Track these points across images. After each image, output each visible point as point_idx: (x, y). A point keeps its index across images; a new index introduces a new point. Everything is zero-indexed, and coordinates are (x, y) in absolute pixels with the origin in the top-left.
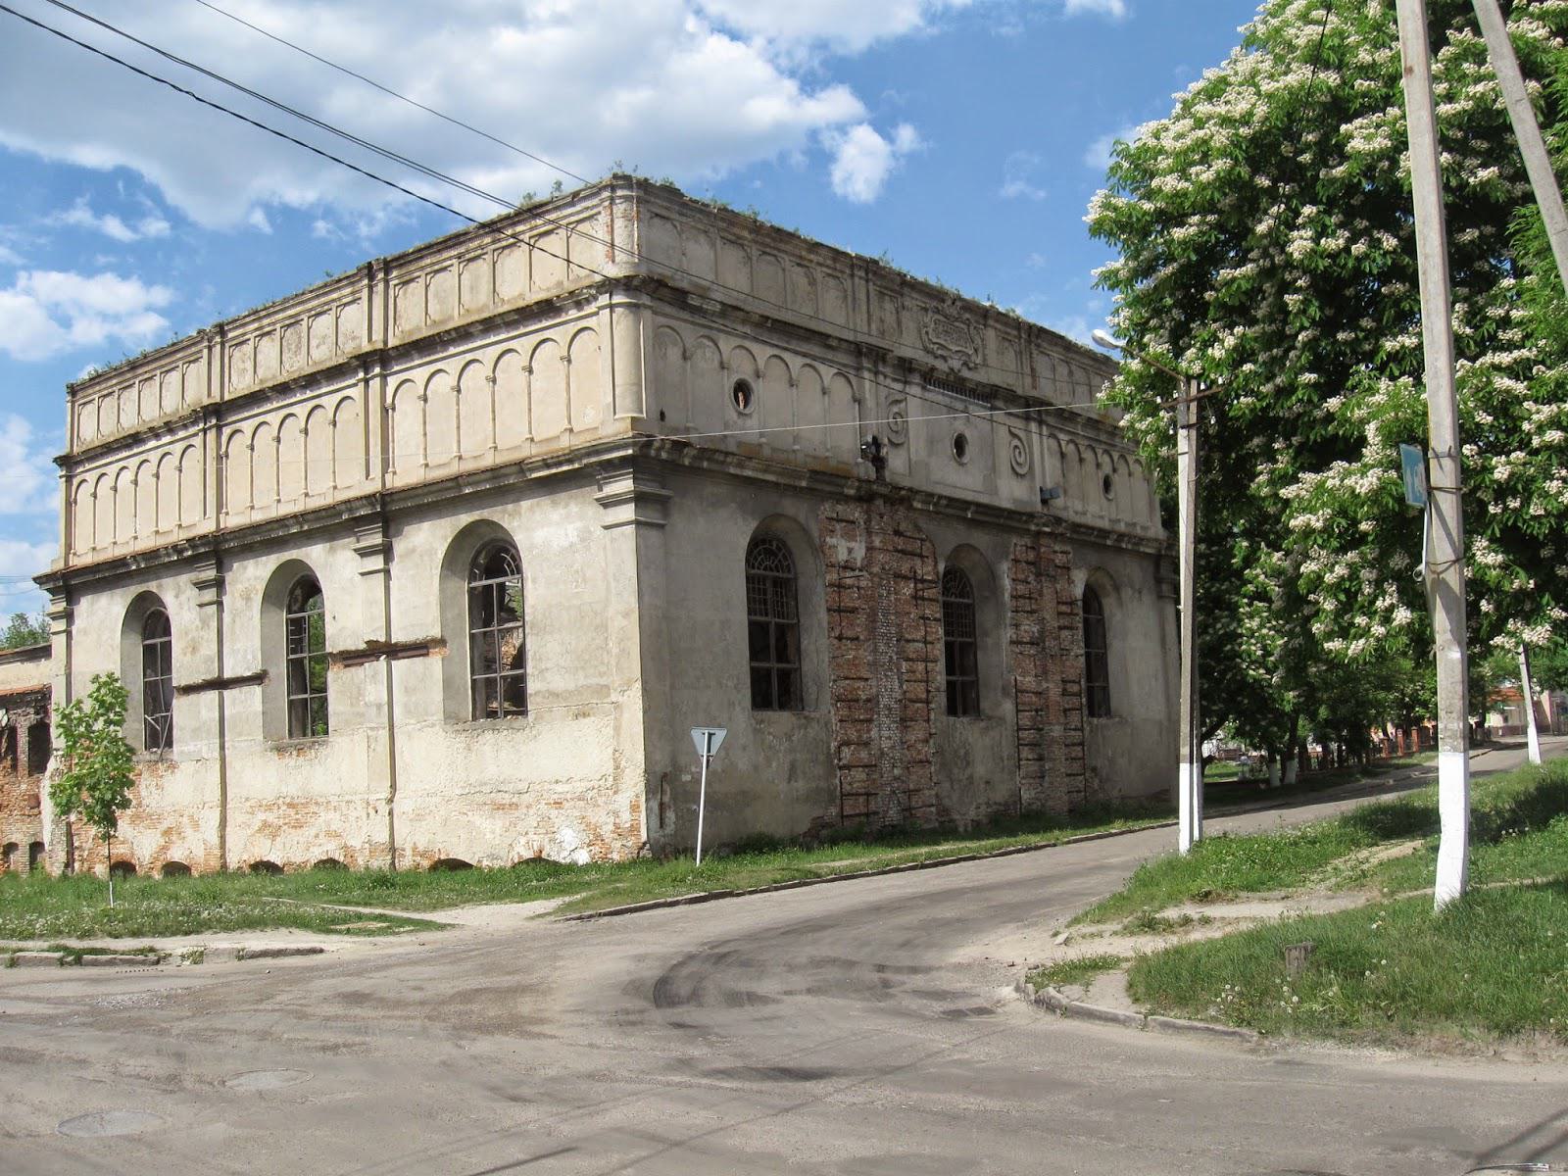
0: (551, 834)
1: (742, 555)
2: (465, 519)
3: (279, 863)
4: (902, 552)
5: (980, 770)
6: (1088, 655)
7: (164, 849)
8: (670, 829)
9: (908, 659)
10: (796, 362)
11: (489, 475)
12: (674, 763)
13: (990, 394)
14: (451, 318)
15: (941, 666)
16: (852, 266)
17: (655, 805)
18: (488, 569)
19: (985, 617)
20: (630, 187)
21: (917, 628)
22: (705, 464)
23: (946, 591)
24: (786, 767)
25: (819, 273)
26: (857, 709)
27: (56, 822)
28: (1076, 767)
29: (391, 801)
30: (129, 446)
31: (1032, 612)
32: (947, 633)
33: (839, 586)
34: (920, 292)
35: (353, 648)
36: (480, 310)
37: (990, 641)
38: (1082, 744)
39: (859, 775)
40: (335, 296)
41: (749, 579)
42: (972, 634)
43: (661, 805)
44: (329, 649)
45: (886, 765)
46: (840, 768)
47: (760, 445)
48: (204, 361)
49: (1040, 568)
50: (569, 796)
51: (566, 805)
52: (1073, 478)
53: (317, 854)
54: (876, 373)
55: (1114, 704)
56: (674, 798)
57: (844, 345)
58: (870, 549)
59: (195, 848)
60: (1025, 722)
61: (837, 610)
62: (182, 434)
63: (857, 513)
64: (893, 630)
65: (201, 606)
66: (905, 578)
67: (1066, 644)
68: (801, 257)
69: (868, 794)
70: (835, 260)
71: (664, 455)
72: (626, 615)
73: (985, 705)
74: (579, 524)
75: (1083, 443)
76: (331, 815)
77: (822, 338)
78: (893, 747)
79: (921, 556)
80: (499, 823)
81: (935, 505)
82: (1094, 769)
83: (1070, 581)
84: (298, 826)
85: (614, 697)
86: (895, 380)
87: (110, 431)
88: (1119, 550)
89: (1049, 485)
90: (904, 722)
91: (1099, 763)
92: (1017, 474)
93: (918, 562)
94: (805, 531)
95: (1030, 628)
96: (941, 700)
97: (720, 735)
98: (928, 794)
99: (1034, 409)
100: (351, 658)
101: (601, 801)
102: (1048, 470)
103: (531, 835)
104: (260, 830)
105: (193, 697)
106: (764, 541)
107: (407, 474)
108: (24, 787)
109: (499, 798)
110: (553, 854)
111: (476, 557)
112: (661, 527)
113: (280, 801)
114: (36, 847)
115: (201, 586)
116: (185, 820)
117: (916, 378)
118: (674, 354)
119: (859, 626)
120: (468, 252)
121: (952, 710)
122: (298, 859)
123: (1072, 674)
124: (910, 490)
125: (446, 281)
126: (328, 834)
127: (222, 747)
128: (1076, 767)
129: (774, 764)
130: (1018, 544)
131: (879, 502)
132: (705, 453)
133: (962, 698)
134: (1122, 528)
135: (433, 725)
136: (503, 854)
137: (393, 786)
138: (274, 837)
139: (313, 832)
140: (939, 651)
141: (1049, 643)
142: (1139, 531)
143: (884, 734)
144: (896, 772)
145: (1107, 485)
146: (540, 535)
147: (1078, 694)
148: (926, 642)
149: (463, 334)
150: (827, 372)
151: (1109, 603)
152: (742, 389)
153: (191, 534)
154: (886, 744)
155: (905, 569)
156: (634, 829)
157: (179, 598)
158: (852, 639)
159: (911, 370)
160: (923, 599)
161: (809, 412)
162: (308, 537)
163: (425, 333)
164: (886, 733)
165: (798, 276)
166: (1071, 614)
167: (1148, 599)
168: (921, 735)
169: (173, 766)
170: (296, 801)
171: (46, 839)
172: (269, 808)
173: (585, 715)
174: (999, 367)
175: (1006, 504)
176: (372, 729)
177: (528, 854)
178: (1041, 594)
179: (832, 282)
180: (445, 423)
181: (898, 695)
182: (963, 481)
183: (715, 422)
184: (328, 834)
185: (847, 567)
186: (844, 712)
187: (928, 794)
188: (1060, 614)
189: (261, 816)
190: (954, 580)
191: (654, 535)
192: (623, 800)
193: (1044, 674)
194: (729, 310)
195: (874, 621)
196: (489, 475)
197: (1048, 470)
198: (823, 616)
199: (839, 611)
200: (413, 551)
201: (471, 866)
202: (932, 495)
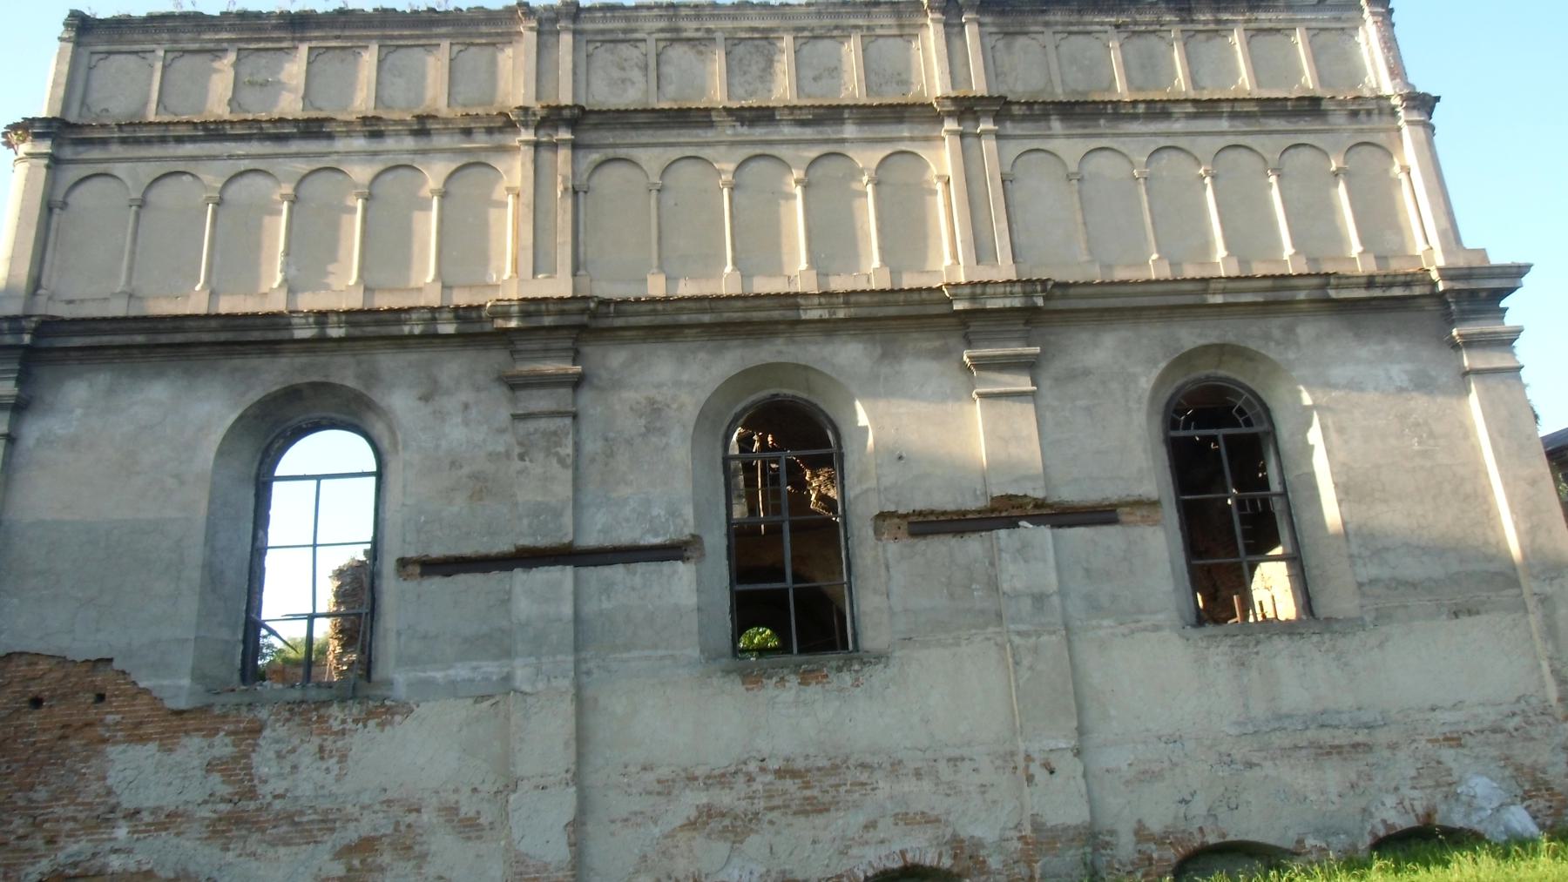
11: (1269, 283)
35: (951, 507)
50: (1471, 727)
51: (1467, 739)
74: (1409, 367)
76: (908, 786)
101: (1536, 732)
103: (1406, 791)
104: (691, 825)
109: (1326, 737)
110: (1457, 820)
113: (753, 767)
120: (1136, 23)
126: (904, 819)
135: (1157, 628)
139: (862, 819)
162: (829, 328)
170: (800, 764)
173: (1470, 613)
176: (1019, 633)
184: (904, 819)
189: (691, 801)
196: (1269, 283)
200: (1086, 372)
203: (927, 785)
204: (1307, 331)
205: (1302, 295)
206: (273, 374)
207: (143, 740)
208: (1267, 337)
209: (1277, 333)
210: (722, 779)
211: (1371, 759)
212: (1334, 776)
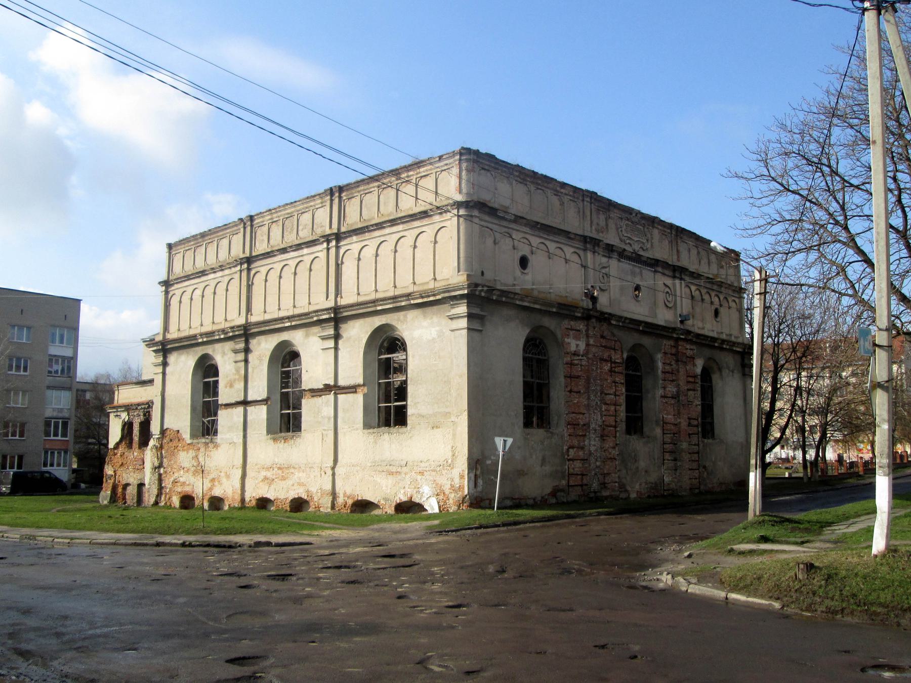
0: (418, 490)
1: (521, 346)
2: (378, 321)
3: (272, 499)
4: (605, 347)
5: (642, 464)
6: (703, 405)
7: (211, 489)
8: (480, 488)
9: (606, 404)
10: (552, 246)
12: (483, 453)
13: (654, 264)
14: (374, 218)
15: (623, 408)
16: (583, 195)
17: (472, 476)
18: (387, 348)
19: (647, 383)
20: (470, 154)
21: (611, 387)
22: (504, 299)
23: (627, 368)
24: (540, 458)
25: (566, 199)
26: (578, 429)
27: (153, 474)
28: (695, 465)
29: (333, 468)
30: (199, 277)
31: (673, 381)
32: (626, 391)
33: (571, 364)
34: (619, 209)
36: (389, 215)
37: (650, 395)
38: (698, 453)
39: (578, 464)
40: (312, 204)
41: (525, 359)
42: (641, 392)
43: (476, 475)
44: (303, 388)
45: (592, 460)
46: (569, 460)
47: (532, 289)
48: (241, 235)
49: (678, 357)
52: (698, 310)
53: (292, 495)
54: (594, 252)
55: (716, 431)
56: (482, 473)
57: (578, 237)
58: (588, 345)
59: (228, 489)
60: (667, 440)
61: (570, 377)
62: (227, 272)
63: (581, 326)
64: (599, 388)
65: (236, 362)
66: (606, 361)
67: (691, 399)
68: (556, 191)
69: (583, 475)
70: (574, 192)
71: (483, 294)
72: (461, 376)
73: (646, 429)
74: (437, 328)
75: (704, 291)
77: (566, 234)
78: (596, 450)
79: (614, 349)
80: (390, 482)
81: (623, 322)
82: (704, 467)
83: (694, 365)
84: (284, 479)
85: (453, 418)
86: (604, 256)
87: (189, 269)
88: (721, 349)
89: (685, 313)
90: (603, 437)
91: (707, 464)
92: (667, 306)
93: (613, 352)
94: (553, 334)
95: (671, 389)
96: (622, 426)
97: (510, 441)
98: (614, 476)
99: (678, 272)
100: (316, 392)
101: (444, 472)
102: (685, 306)
103: (406, 489)
105: (229, 410)
106: (532, 339)
107: (348, 297)
108: (135, 454)
111: (383, 342)
112: (481, 331)
114: (141, 486)
115: (236, 352)
116: (222, 474)
117: (615, 255)
118: (490, 241)
119: (581, 385)
121: (629, 431)
122: (282, 496)
123: (694, 415)
124: (610, 314)
125: (371, 200)
126: (301, 484)
127: (245, 436)
128: (695, 465)
129: (534, 457)
130: (667, 344)
131: (594, 320)
132: (503, 293)
133: (635, 425)
134: (724, 337)
135: (357, 429)
136: (392, 498)
137: (336, 461)
138: (270, 485)
139: (291, 483)
140: (622, 400)
141: (682, 398)
142: (733, 339)
143: (593, 443)
144: (598, 464)
145: (716, 313)
146: (417, 333)
147: (697, 426)
148: (615, 395)
149: (380, 226)
150: (569, 251)
151: (715, 377)
152: (524, 262)
153: (232, 324)
154: (593, 449)
155: (606, 356)
156: (461, 488)
157: (226, 359)
158: (577, 392)
159: (612, 251)
160: (615, 372)
161: (559, 274)
163: (360, 226)
164: (593, 443)
165: (555, 200)
166: (694, 382)
167: (737, 375)
168: (611, 445)
169: (216, 446)
171: (147, 482)
172: (268, 469)
174: (660, 250)
175: (662, 323)
177: (404, 499)
178: (678, 371)
179: (572, 204)
180: (370, 271)
181: (600, 422)
182: (638, 311)
183: (508, 276)
184: (301, 484)
185: (575, 354)
186: (571, 431)
187: (614, 476)
188: (688, 382)
190: (632, 363)
191: (476, 334)
192: (456, 473)
193: (678, 414)
194: (518, 219)
195: (589, 383)
197: (685, 306)
198: (562, 379)
199: (570, 377)
200: (350, 338)
201: (372, 503)
202: (621, 317)
203: (304, 474)
204: (412, 314)
205: (403, 304)
206: (200, 351)
207: (183, 450)
208: (399, 320)
209: (402, 317)
210: (268, 469)
211: (399, 477)
212: (391, 480)
